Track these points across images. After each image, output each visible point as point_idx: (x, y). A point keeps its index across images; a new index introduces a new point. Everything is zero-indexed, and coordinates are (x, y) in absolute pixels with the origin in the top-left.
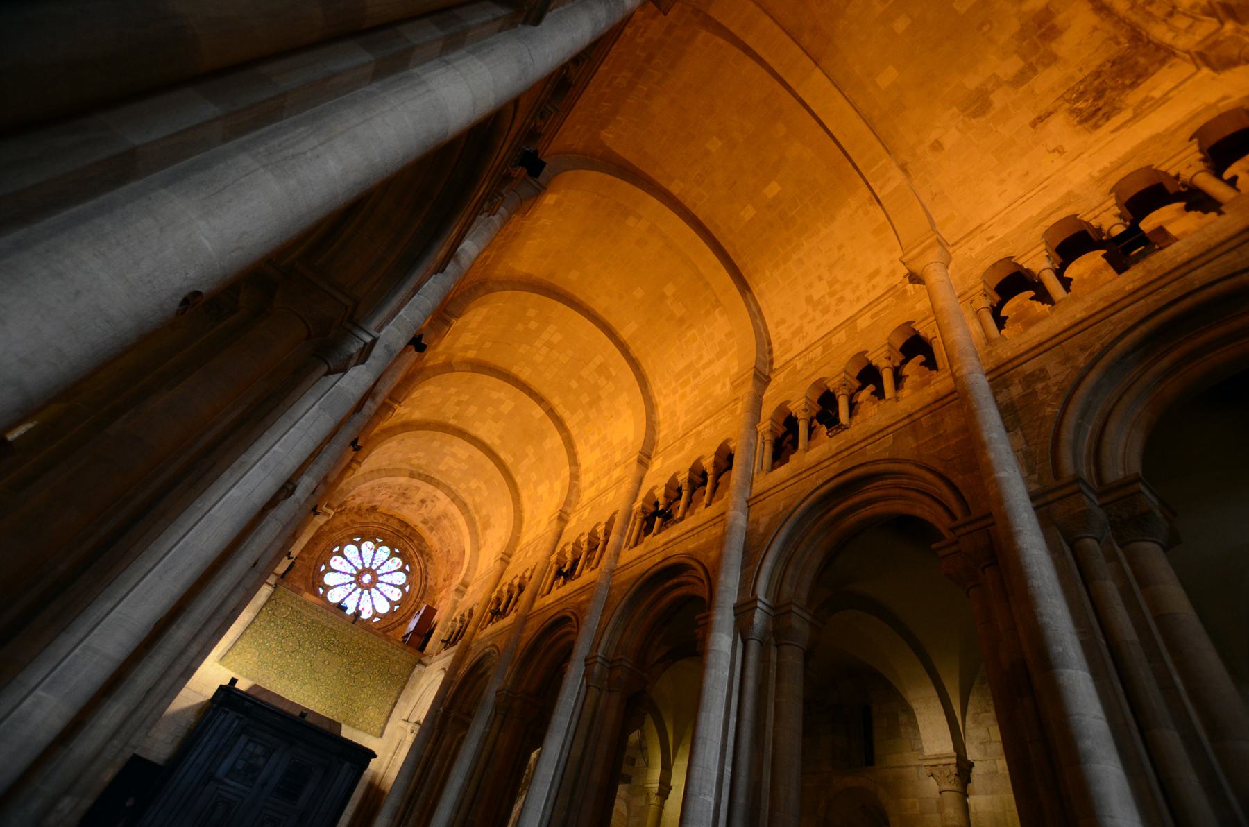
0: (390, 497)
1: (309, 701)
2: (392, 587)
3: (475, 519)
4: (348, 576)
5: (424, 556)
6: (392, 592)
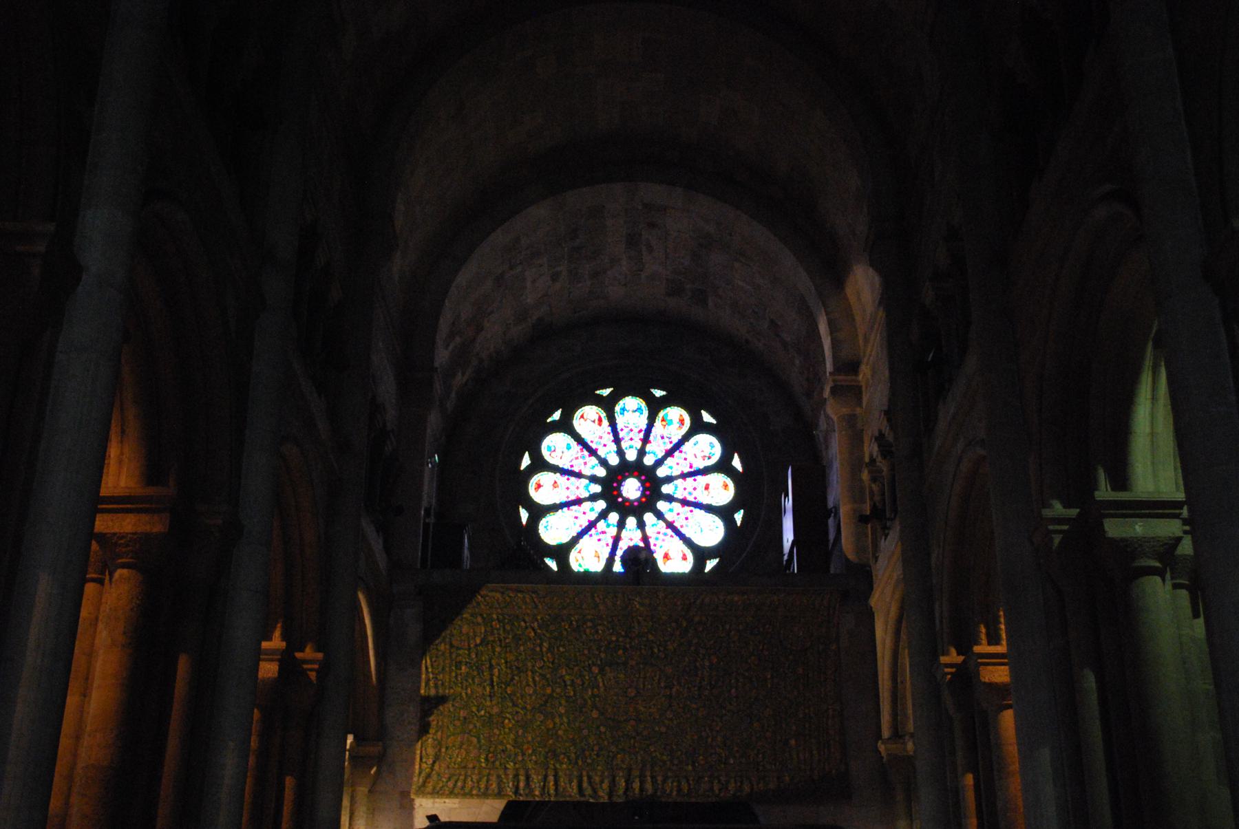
2: (699, 478)
6: (707, 487)
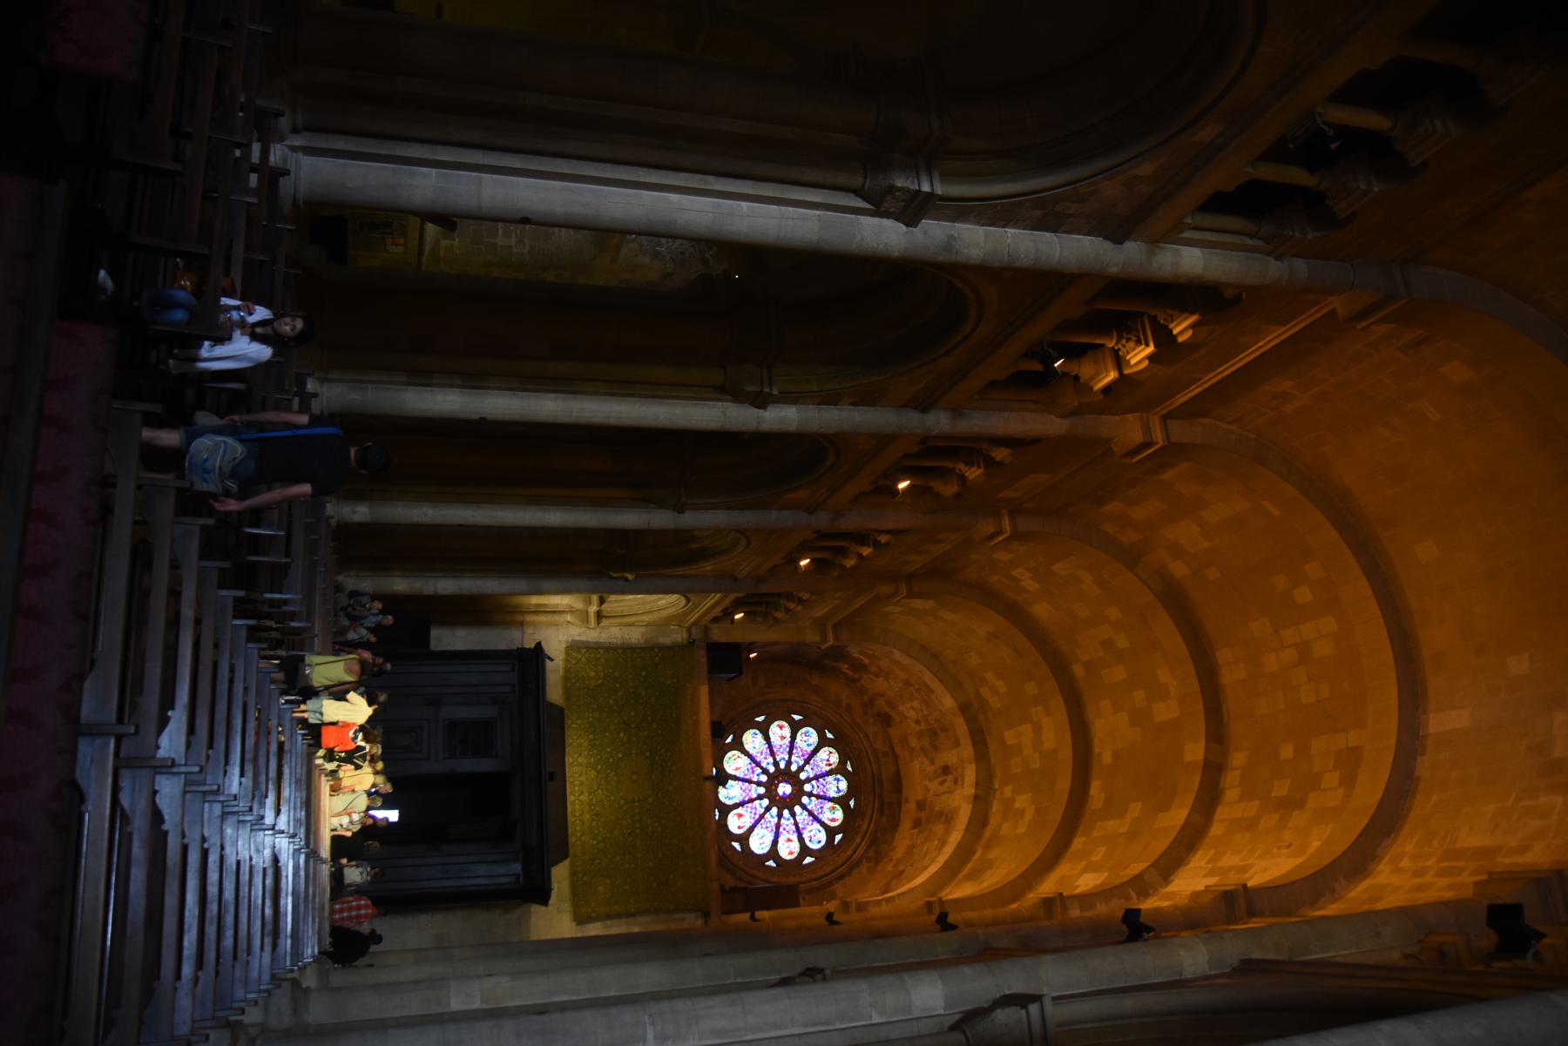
0: (917, 722)
1: (577, 788)
3: (974, 854)
4: (771, 760)
6: (789, 840)
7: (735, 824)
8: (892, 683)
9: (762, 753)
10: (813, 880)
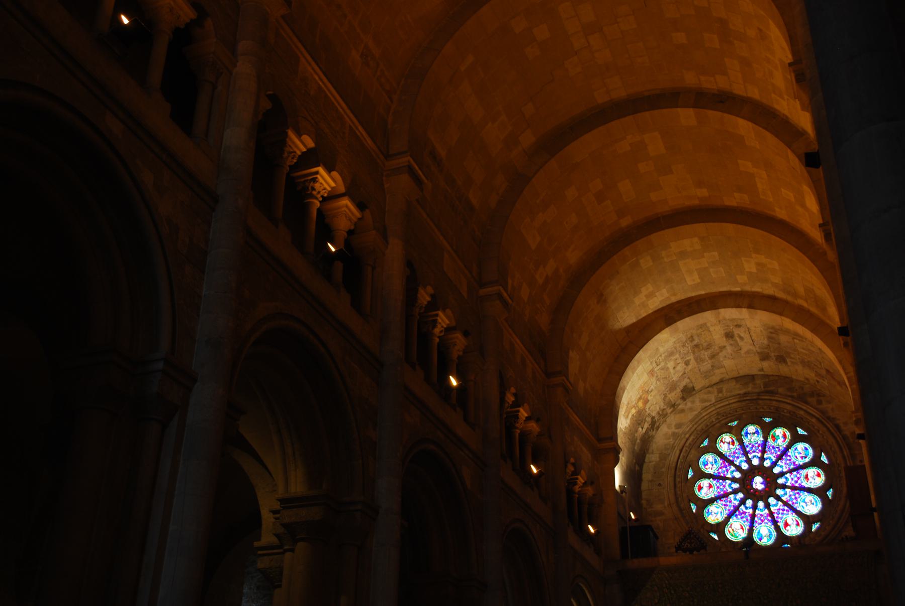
3: (803, 306)
5: (810, 400)
6: (807, 477)
7: (794, 529)
8: (652, 387)
9: (726, 505)
10: (842, 452)
